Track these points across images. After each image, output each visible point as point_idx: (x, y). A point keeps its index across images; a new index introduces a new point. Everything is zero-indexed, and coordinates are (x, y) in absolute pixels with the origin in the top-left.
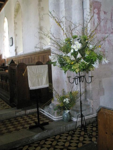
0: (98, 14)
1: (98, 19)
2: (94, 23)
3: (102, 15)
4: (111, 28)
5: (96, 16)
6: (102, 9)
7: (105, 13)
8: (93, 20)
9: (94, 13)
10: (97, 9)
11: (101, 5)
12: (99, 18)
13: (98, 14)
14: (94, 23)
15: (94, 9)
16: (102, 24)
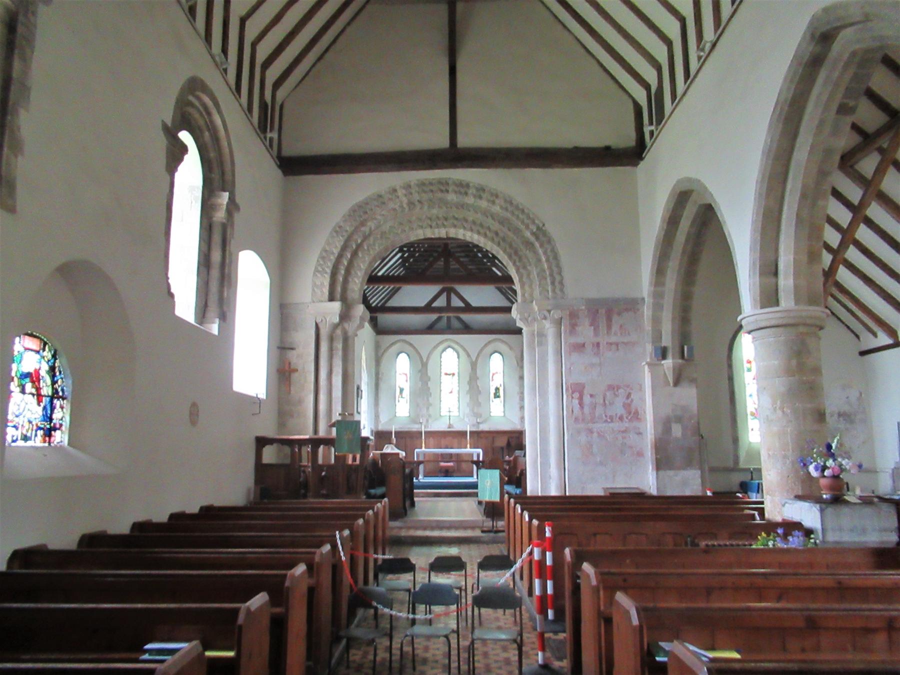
0: (581, 399)
1: (579, 406)
2: (572, 411)
3: (587, 399)
4: (604, 415)
5: (576, 402)
6: (585, 392)
7: (591, 396)
8: (571, 408)
9: (572, 398)
10: (578, 393)
11: (584, 387)
12: (581, 404)
13: (581, 399)
14: (572, 411)
15: (573, 393)
16: (587, 410)
